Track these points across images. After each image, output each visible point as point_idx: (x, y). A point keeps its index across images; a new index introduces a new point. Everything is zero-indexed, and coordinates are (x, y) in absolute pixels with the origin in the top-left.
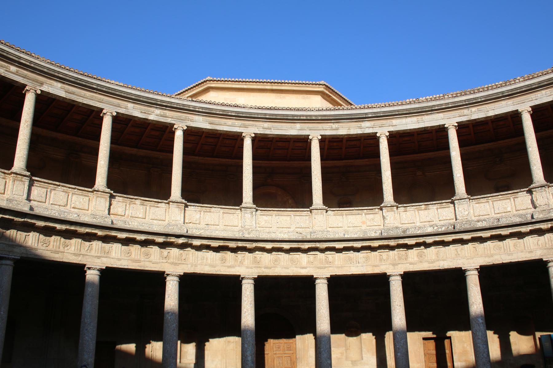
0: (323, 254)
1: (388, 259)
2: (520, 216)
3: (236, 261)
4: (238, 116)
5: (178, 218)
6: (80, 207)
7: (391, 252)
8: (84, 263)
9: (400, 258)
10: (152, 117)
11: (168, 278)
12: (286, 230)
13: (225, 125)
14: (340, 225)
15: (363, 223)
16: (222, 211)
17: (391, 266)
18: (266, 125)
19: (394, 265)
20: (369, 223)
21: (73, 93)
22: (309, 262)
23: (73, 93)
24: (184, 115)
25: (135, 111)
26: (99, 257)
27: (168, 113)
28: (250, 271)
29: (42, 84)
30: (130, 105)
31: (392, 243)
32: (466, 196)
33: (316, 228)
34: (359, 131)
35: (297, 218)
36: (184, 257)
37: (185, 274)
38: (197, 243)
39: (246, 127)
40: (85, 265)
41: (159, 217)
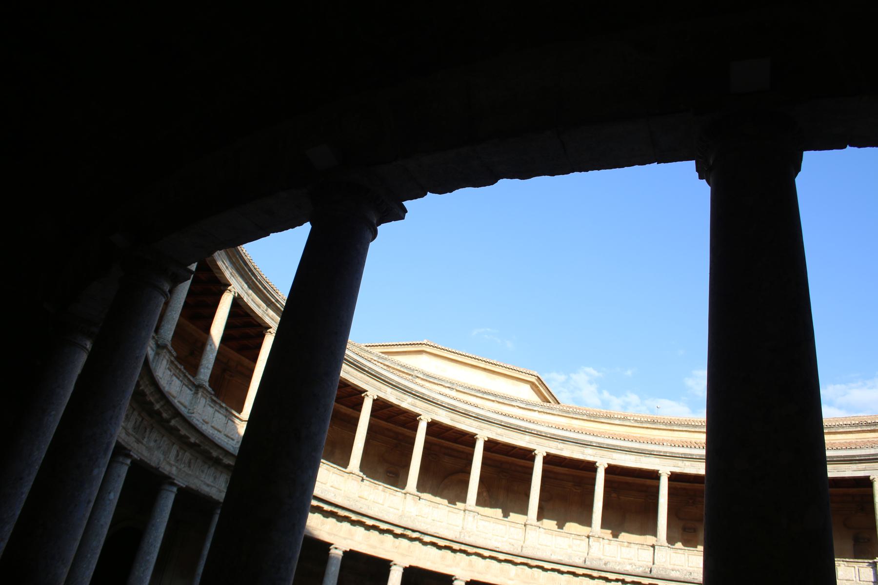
0: (530, 570)
4: (477, 418)
7: (591, 581)
8: (331, 542)
11: (393, 568)
13: (464, 423)
15: (570, 546)
25: (392, 396)
26: (345, 539)
27: (419, 403)
30: (389, 390)
31: (595, 574)
32: (667, 544)
37: (411, 567)
38: (427, 539)
40: (332, 544)
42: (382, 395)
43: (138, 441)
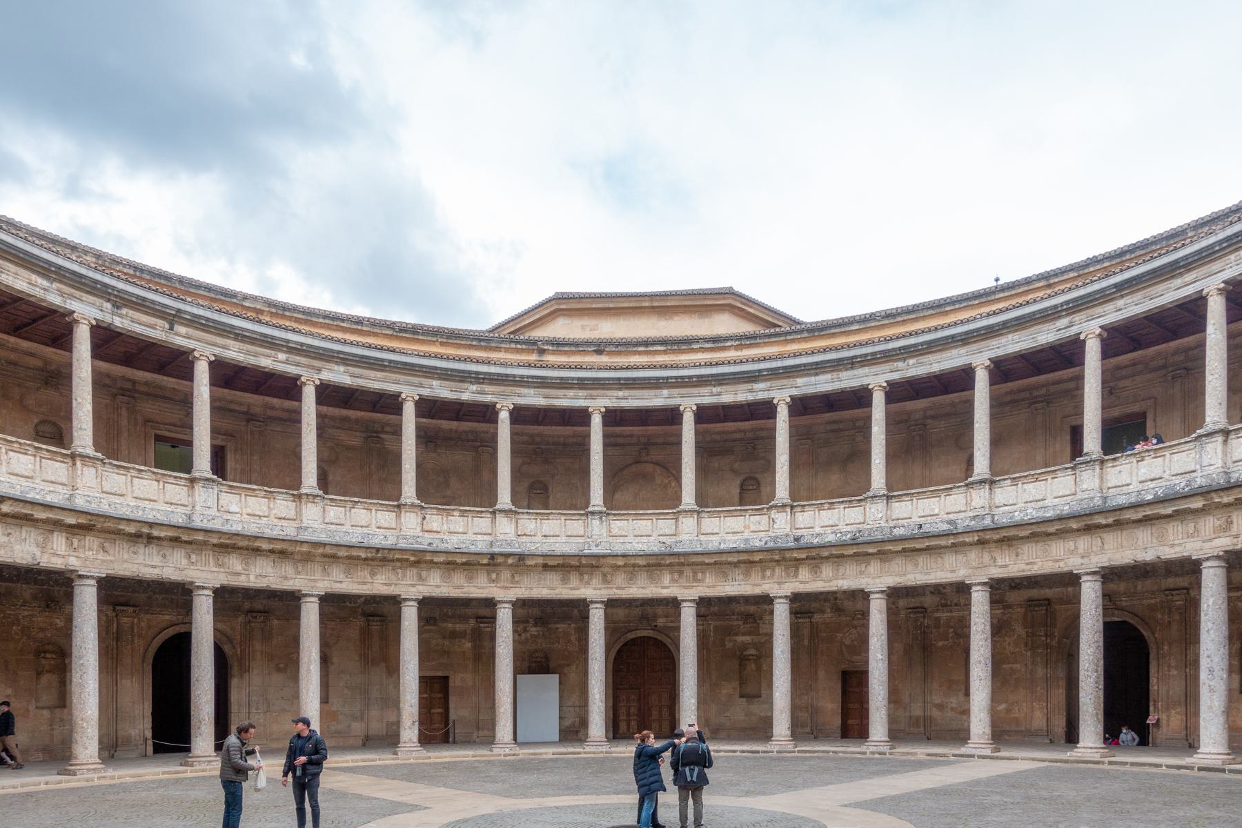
2: (949, 522)
3: (581, 580)
6: (387, 525)
9: (788, 575)
12: (645, 539)
16: (563, 518)
20: (753, 528)
22: (673, 580)
26: (413, 586)
28: (598, 592)
36: (517, 578)
41: (484, 530)
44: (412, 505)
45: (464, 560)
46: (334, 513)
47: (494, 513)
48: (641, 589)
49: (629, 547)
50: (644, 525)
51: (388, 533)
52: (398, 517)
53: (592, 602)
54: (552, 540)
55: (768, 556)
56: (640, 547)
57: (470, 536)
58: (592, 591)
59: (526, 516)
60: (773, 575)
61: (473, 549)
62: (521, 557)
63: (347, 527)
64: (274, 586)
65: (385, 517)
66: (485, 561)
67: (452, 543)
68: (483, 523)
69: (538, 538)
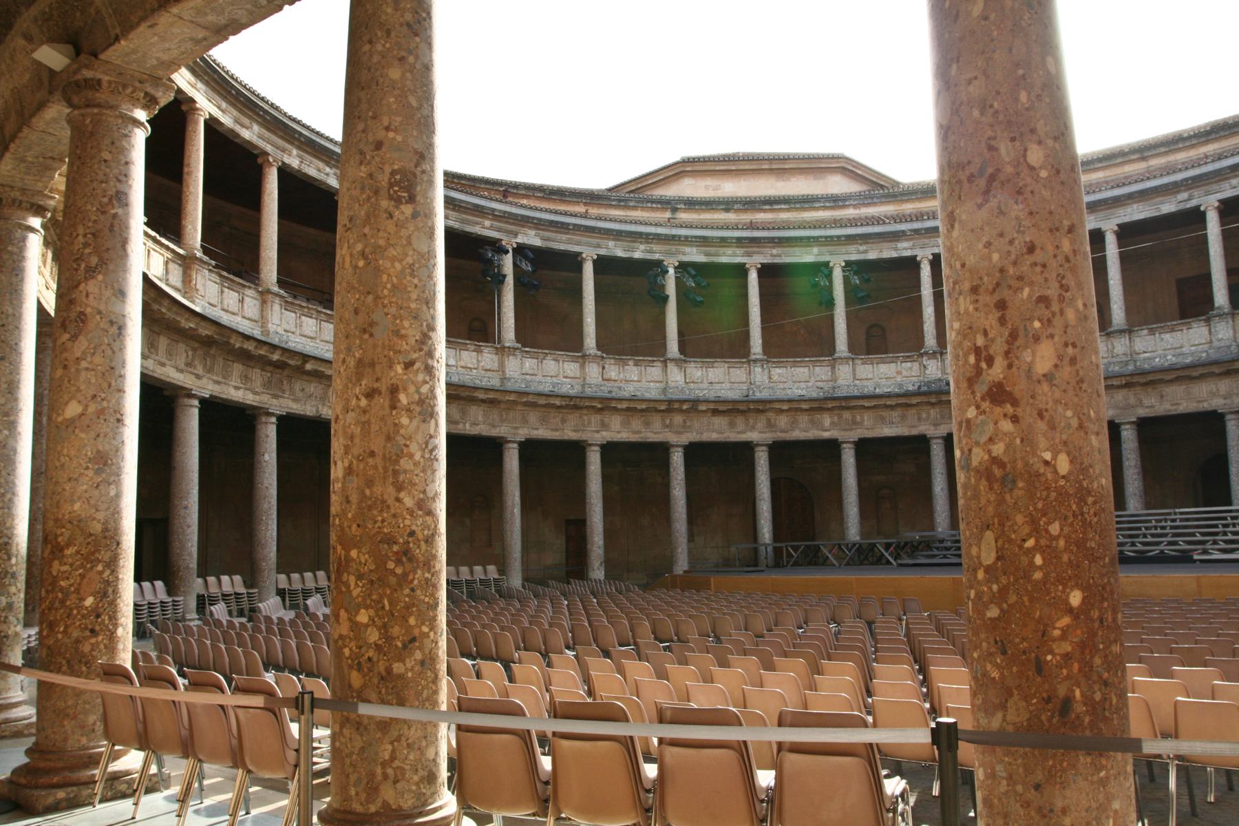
1: (928, 418)
5: (678, 378)
9: (943, 417)
10: (637, 255)
12: (803, 385)
13: (724, 254)
14: (870, 376)
17: (932, 428)
18: (775, 251)
19: (936, 425)
20: (905, 373)
21: (548, 239)
22: (832, 423)
23: (548, 239)
24: (673, 248)
25: (618, 250)
26: (598, 432)
27: (655, 247)
28: (764, 435)
29: (516, 235)
30: (611, 244)
33: (840, 382)
34: (894, 255)
35: (817, 369)
39: (749, 255)
41: (656, 378)
42: (603, 252)
43: (275, 396)
44: (596, 356)
45: (644, 407)
46: (529, 364)
47: (665, 362)
48: (803, 431)
49: (789, 392)
50: (801, 372)
51: (574, 382)
52: (582, 367)
53: (758, 445)
54: (717, 386)
55: (924, 399)
56: (800, 392)
57: (644, 384)
58: (756, 433)
59: (693, 365)
60: (928, 418)
61: (647, 396)
62: (695, 402)
63: (539, 378)
64: (484, 433)
65: (571, 368)
66: (663, 408)
67: (629, 390)
68: (655, 371)
69: (705, 385)
